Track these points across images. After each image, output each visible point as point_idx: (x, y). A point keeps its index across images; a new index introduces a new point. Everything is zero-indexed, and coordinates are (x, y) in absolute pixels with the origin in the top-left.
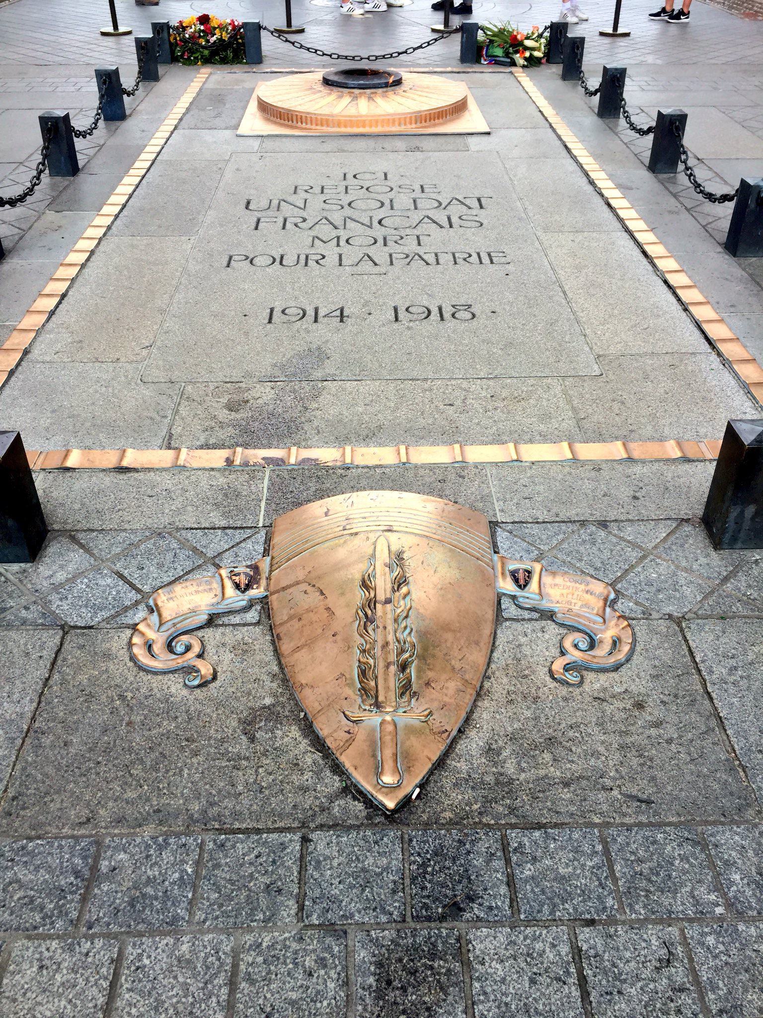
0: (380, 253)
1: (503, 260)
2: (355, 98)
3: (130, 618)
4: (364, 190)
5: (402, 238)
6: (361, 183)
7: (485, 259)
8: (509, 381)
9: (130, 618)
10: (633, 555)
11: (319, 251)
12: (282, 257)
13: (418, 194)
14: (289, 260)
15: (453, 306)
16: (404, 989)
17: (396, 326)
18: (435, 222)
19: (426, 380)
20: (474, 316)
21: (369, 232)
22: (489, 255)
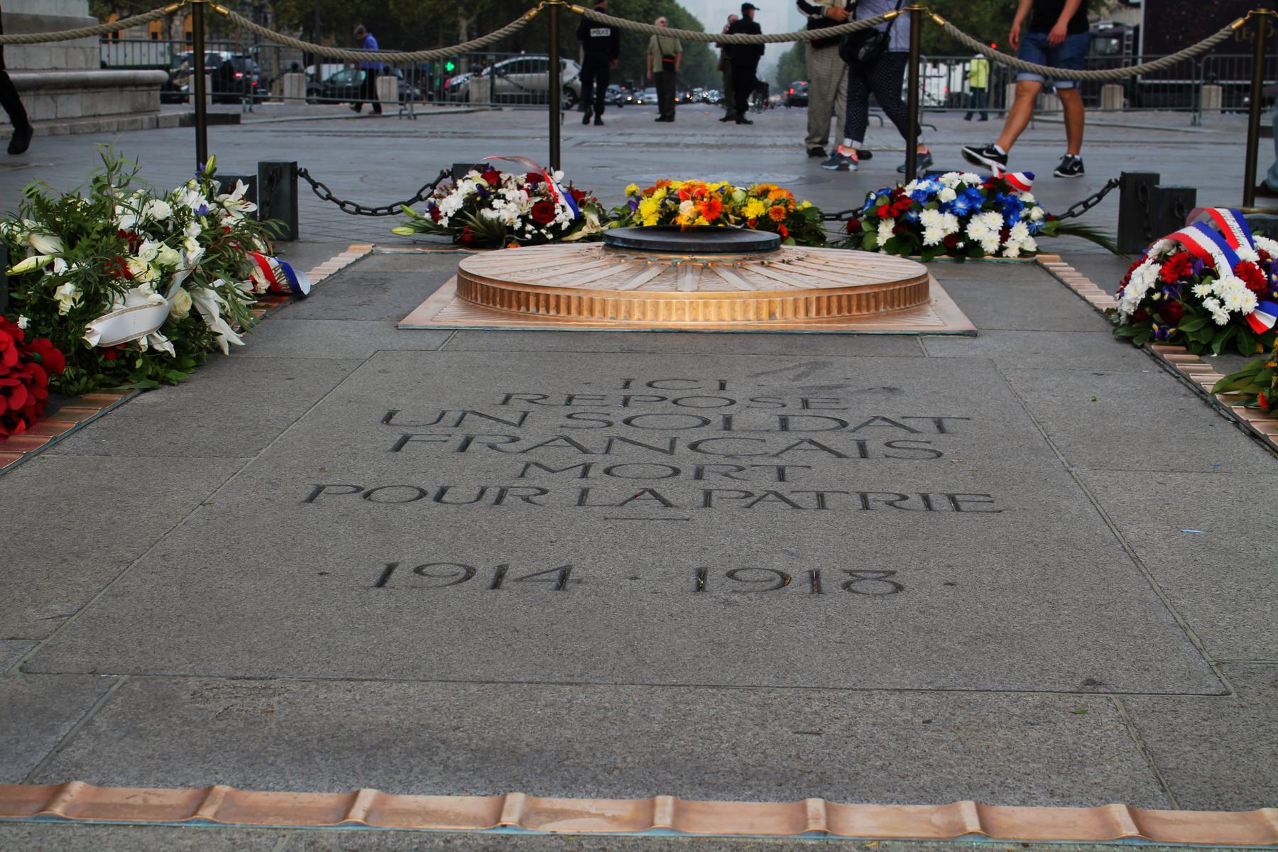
2: (676, 270)
4: (668, 403)
5: (741, 469)
6: (661, 393)
7: (941, 503)
8: (976, 696)
11: (537, 483)
12: (443, 491)
13: (793, 407)
15: (851, 573)
18: (823, 448)
19: (753, 688)
20: (899, 588)
22: (952, 498)
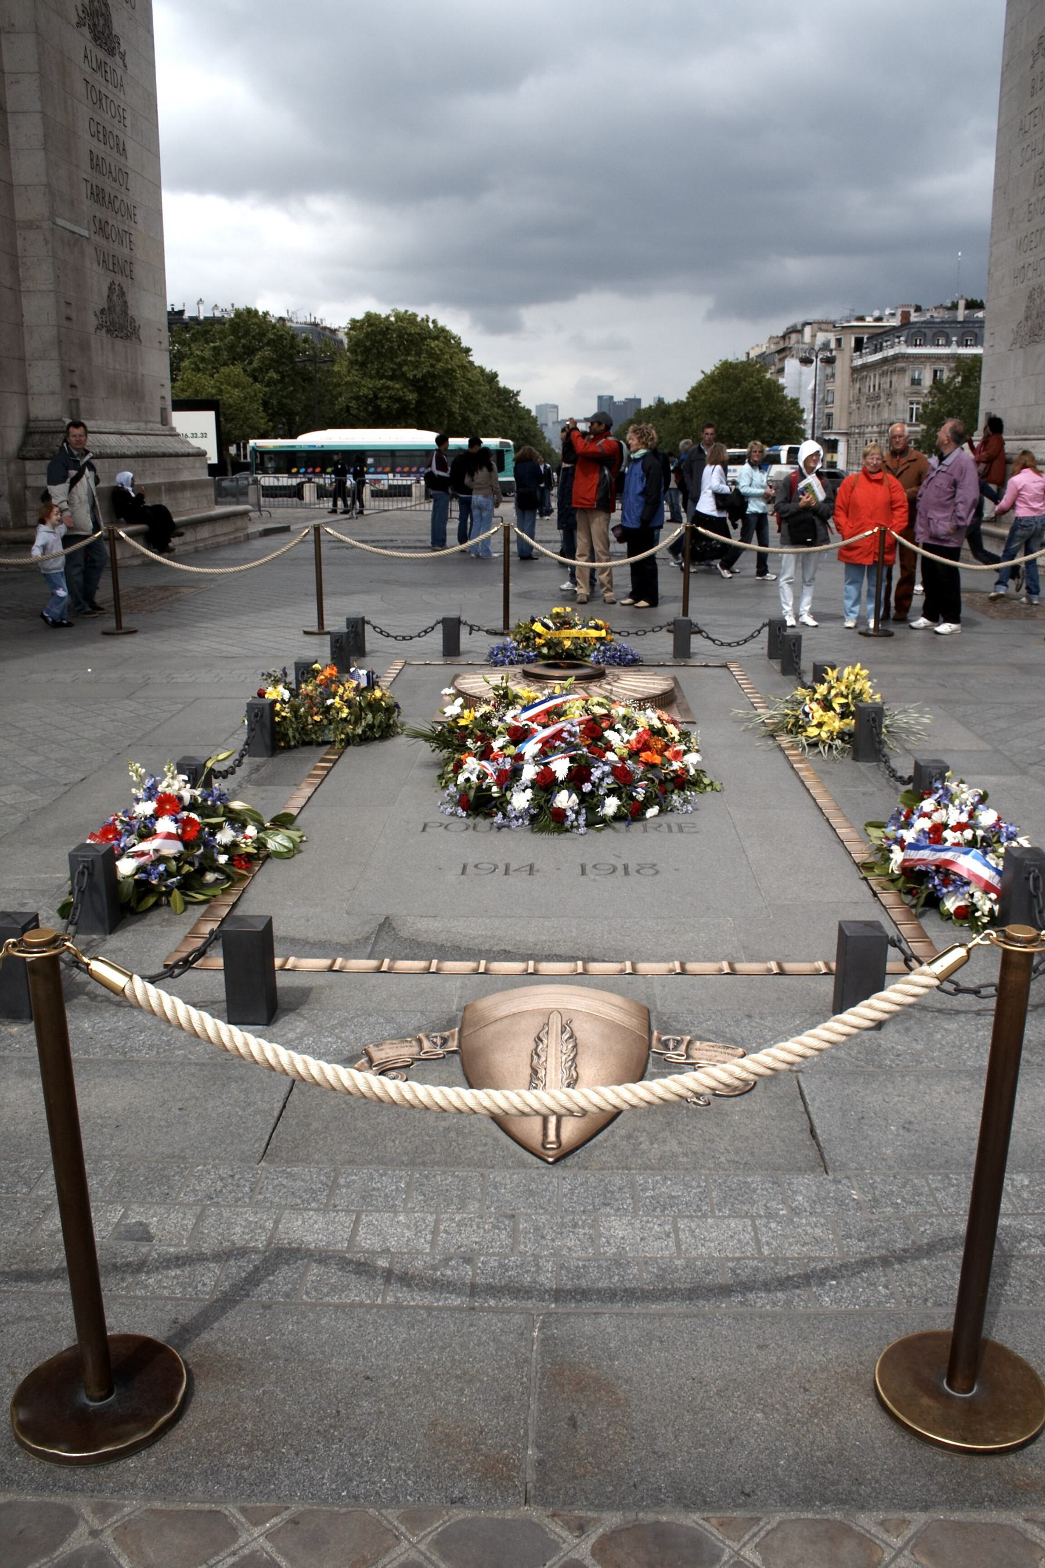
1: (693, 830)
7: (675, 828)
15: (639, 865)
16: (553, 1240)
17: (582, 879)
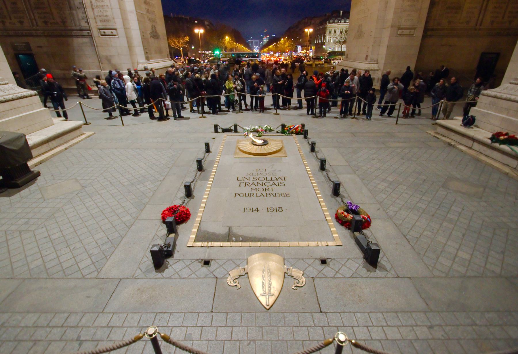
0: (264, 193)
3: (226, 277)
9: (226, 277)
10: (307, 265)
14: (247, 195)
21: (262, 187)
